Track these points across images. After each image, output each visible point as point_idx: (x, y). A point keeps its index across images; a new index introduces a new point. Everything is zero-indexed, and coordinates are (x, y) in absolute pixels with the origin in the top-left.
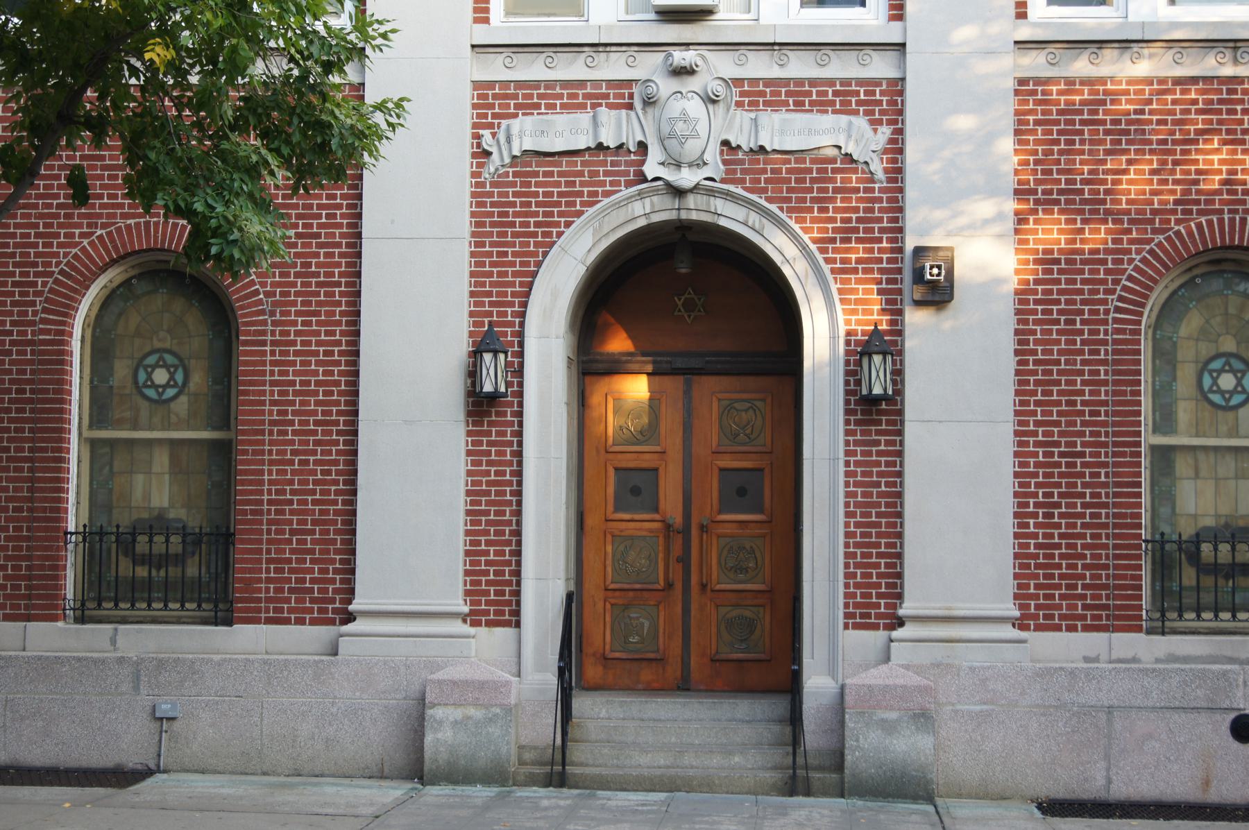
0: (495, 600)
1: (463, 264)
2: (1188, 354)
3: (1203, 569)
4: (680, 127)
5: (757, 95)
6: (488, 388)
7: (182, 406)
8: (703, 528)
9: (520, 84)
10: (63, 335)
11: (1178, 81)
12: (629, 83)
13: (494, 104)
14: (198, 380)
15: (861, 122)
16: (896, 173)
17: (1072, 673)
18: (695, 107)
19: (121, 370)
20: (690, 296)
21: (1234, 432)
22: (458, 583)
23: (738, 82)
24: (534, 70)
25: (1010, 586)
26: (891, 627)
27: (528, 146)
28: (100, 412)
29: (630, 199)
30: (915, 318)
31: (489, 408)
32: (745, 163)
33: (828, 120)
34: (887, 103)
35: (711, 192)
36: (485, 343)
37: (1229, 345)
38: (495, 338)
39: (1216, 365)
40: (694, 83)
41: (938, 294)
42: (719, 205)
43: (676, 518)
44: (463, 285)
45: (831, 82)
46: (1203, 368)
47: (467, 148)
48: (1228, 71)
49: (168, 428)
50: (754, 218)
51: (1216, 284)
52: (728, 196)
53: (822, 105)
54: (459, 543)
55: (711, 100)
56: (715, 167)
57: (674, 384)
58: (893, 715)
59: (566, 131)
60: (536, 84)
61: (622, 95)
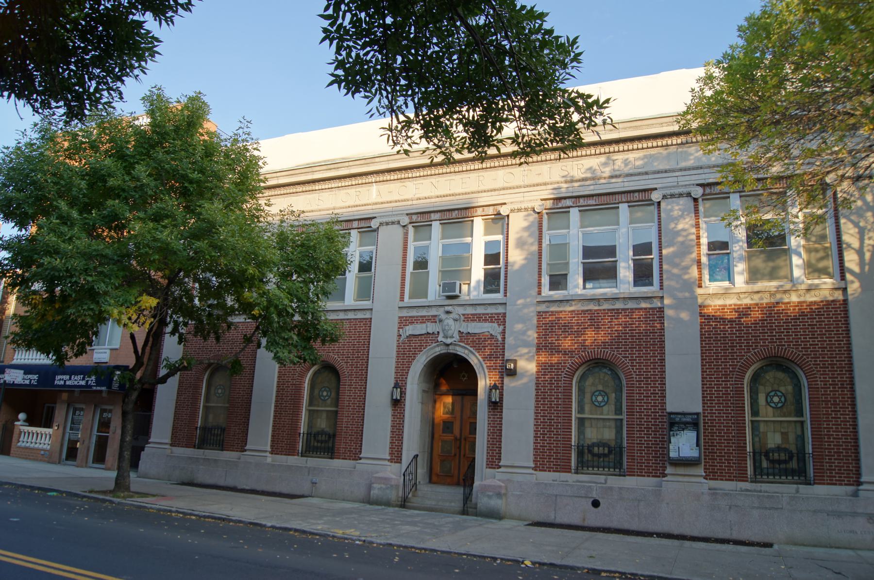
0: (396, 456)
1: (394, 365)
2: (589, 390)
3: (594, 455)
4: (447, 328)
5: (468, 318)
6: (493, 400)
7: (329, 401)
8: (465, 439)
9: (410, 317)
10: (302, 383)
11: (582, 311)
12: (436, 316)
13: (404, 322)
14: (333, 395)
15: (495, 325)
16: (504, 339)
17: (546, 484)
18: (451, 322)
19: (316, 392)
20: (450, 373)
21: (602, 414)
22: (388, 450)
23: (464, 315)
24: (414, 313)
25: (532, 458)
26: (664, 477)
27: (411, 333)
28: (311, 402)
29: (435, 347)
30: (506, 380)
31: (397, 403)
32: (465, 337)
33: (487, 324)
34: (501, 319)
35: (455, 345)
36: (396, 386)
37: (600, 388)
38: (400, 385)
39: (597, 393)
40: (451, 316)
41: (512, 373)
42: (458, 348)
43: (458, 437)
44: (393, 370)
45: (488, 314)
46: (593, 394)
47: (396, 334)
48: (596, 308)
49: (325, 406)
50: (466, 351)
51: (597, 370)
52: (460, 346)
53: (486, 320)
54: (388, 440)
55: (455, 320)
56: (457, 337)
57: (459, 398)
58: (491, 494)
59: (419, 329)
60: (413, 317)
61: (433, 319)
